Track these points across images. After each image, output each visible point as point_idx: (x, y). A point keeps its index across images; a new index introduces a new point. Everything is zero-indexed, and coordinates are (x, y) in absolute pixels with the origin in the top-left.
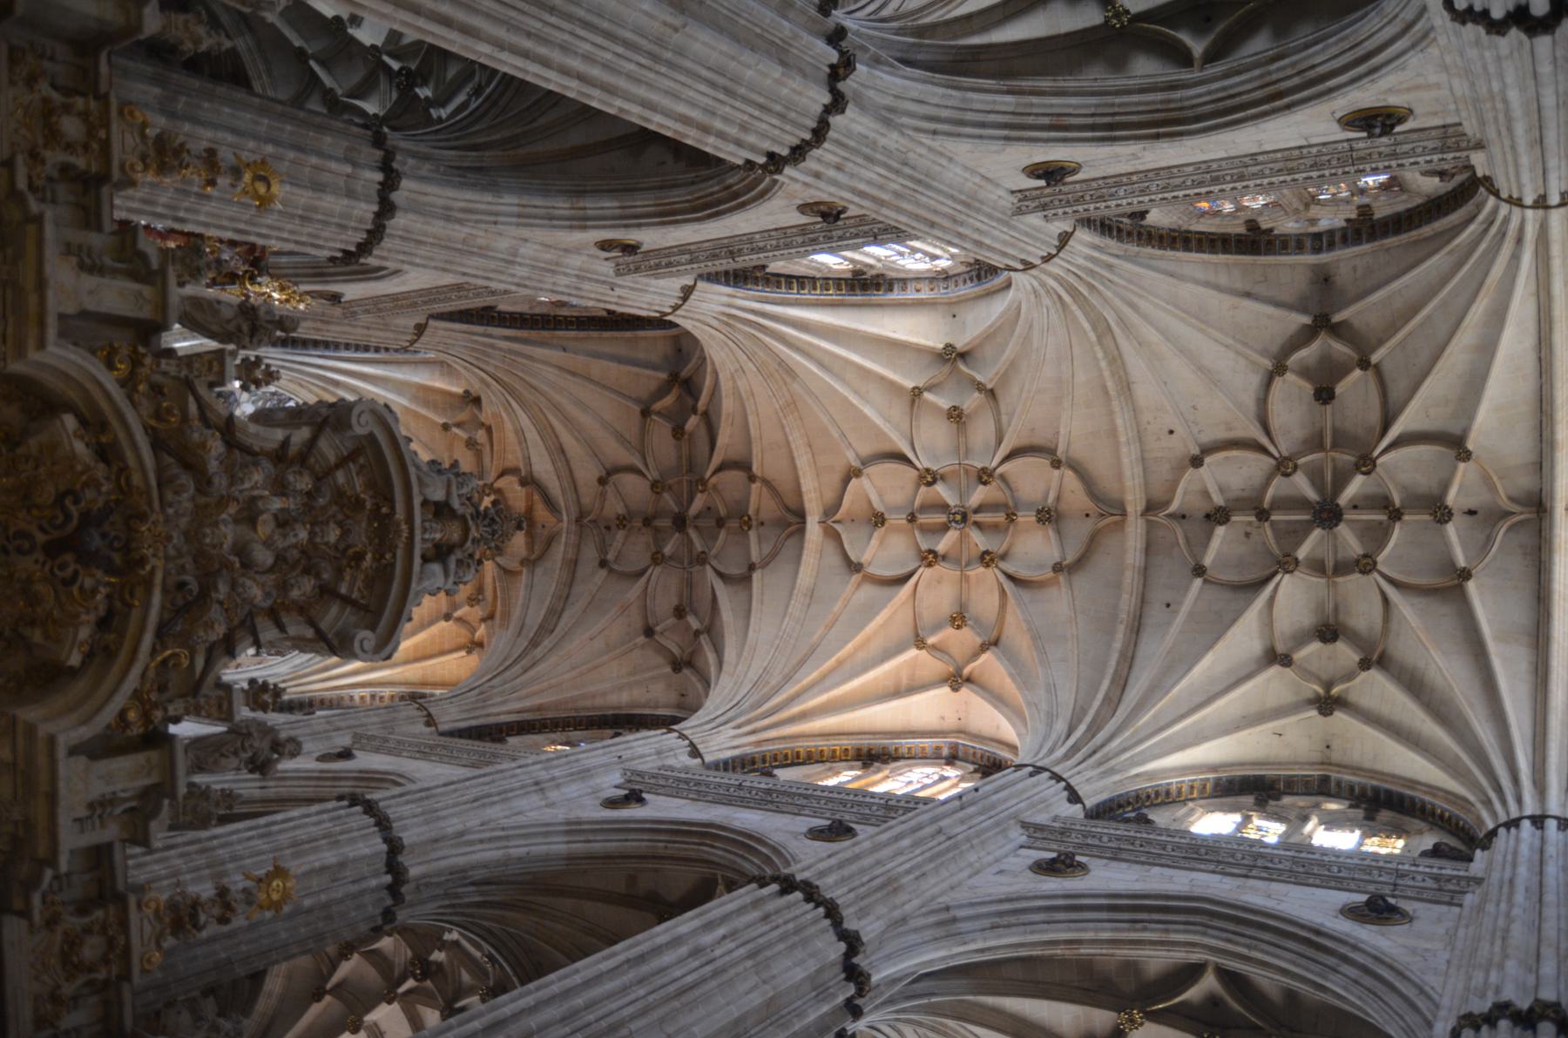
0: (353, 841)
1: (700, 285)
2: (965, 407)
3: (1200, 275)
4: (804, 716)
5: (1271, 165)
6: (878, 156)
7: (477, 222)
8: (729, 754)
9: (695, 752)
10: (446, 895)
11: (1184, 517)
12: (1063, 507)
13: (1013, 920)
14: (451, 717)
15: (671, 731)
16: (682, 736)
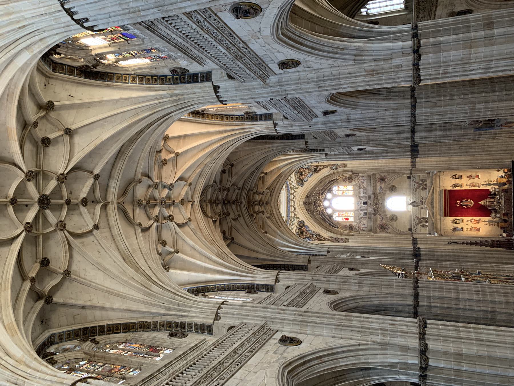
0: (425, 113)
1: (273, 283)
2: (162, 246)
3: (111, 314)
4: (220, 132)
5: (228, 364)
6: (379, 332)
7: (381, 294)
8: (259, 123)
9: (275, 125)
10: (390, 92)
11: (93, 202)
12: (131, 207)
13: (335, 50)
14: (299, 144)
15: (277, 133)
16: (276, 130)
